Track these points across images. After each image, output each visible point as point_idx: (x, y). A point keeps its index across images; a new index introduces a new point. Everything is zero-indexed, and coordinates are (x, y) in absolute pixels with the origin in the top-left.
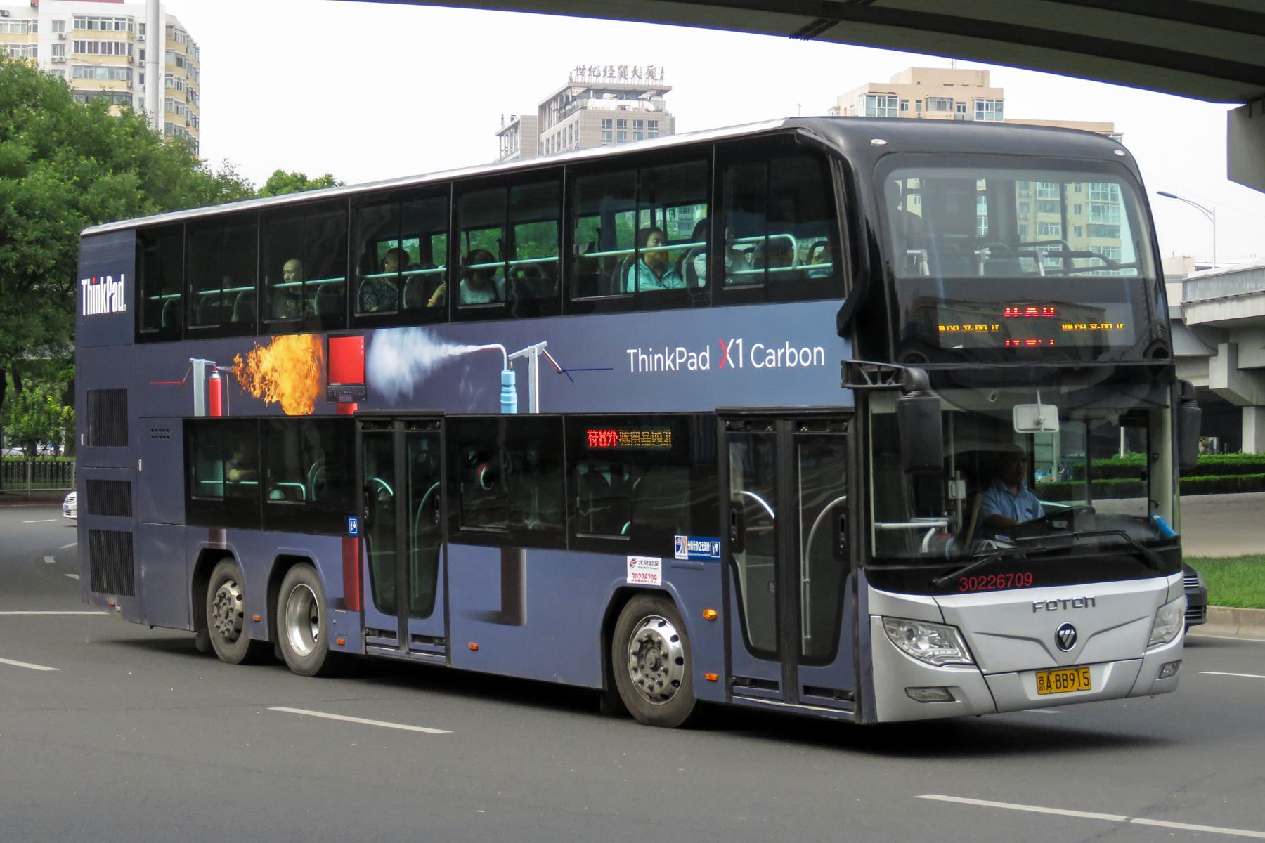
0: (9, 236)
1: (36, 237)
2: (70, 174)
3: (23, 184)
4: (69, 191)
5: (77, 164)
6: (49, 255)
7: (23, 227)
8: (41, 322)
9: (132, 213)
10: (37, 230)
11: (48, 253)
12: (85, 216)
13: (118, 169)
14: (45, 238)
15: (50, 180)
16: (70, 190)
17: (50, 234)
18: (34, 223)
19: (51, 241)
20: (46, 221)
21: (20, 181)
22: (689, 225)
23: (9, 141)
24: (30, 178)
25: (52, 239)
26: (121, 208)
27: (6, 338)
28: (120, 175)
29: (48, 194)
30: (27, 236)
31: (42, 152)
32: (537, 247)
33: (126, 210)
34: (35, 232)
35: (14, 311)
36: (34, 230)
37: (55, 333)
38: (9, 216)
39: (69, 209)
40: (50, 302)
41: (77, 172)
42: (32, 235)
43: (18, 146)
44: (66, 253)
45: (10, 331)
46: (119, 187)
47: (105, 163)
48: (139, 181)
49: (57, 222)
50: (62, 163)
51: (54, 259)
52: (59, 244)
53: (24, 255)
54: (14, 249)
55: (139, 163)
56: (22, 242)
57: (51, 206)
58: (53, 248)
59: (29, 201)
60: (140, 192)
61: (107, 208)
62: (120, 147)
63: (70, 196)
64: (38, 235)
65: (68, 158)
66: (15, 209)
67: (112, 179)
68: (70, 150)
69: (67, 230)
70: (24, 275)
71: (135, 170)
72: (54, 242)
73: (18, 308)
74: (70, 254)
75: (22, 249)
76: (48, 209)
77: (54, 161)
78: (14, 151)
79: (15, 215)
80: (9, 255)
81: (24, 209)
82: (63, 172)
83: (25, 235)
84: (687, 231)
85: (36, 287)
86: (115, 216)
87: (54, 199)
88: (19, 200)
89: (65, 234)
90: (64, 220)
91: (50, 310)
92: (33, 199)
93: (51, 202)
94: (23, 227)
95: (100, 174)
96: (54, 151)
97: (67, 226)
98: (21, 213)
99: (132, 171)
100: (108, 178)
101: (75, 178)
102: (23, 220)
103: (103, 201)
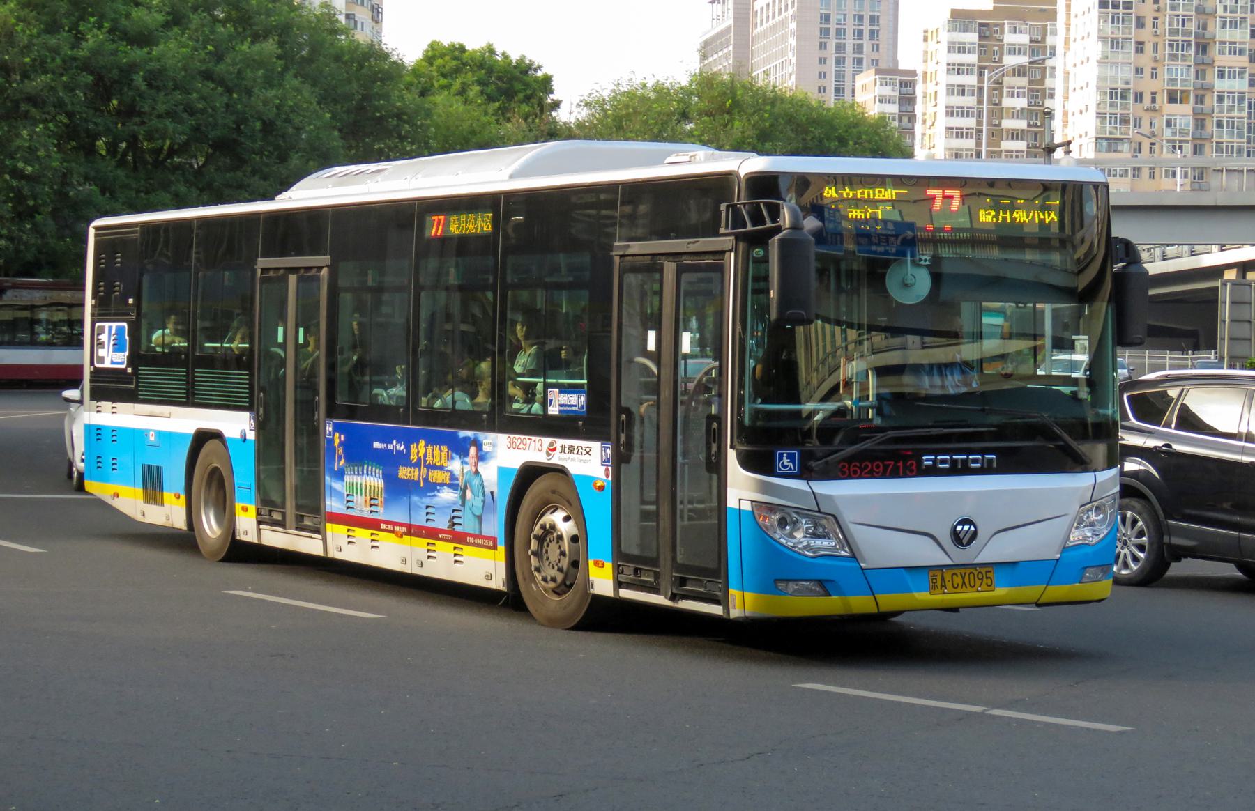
0: (137, 109)
2: (207, 41)
3: (154, 53)
4: (203, 61)
5: (213, 32)
7: (154, 100)
11: (180, 128)
13: (256, 38)
15: (184, 50)
16: (205, 59)
18: (166, 95)
21: (151, 49)
23: (140, 7)
24: (161, 47)
25: (183, 112)
26: (259, 80)
28: (258, 45)
29: (179, 65)
31: (176, 20)
40: (181, 179)
41: (212, 40)
42: (161, 108)
43: (150, 12)
46: (256, 57)
47: (244, 30)
48: (279, 51)
49: (189, 94)
50: (196, 30)
51: (186, 134)
54: (143, 123)
55: (280, 31)
56: (151, 115)
57: (184, 77)
59: (159, 69)
60: (281, 62)
61: (243, 79)
62: (260, 14)
63: (204, 68)
65: (203, 26)
66: (145, 79)
67: (249, 48)
68: (205, 17)
71: (274, 40)
72: (185, 115)
74: (203, 128)
75: (151, 123)
77: (189, 29)
78: (148, 19)
79: (143, 87)
80: (135, 128)
81: (155, 79)
82: (197, 41)
85: (169, 161)
86: (252, 87)
87: (186, 71)
88: (148, 71)
90: (197, 92)
92: (166, 70)
93: (183, 73)
94: (154, 100)
95: (237, 43)
96: (189, 17)
98: (150, 85)
99: (271, 40)
100: (245, 47)
101: (210, 48)
102: (153, 91)
103: (239, 72)
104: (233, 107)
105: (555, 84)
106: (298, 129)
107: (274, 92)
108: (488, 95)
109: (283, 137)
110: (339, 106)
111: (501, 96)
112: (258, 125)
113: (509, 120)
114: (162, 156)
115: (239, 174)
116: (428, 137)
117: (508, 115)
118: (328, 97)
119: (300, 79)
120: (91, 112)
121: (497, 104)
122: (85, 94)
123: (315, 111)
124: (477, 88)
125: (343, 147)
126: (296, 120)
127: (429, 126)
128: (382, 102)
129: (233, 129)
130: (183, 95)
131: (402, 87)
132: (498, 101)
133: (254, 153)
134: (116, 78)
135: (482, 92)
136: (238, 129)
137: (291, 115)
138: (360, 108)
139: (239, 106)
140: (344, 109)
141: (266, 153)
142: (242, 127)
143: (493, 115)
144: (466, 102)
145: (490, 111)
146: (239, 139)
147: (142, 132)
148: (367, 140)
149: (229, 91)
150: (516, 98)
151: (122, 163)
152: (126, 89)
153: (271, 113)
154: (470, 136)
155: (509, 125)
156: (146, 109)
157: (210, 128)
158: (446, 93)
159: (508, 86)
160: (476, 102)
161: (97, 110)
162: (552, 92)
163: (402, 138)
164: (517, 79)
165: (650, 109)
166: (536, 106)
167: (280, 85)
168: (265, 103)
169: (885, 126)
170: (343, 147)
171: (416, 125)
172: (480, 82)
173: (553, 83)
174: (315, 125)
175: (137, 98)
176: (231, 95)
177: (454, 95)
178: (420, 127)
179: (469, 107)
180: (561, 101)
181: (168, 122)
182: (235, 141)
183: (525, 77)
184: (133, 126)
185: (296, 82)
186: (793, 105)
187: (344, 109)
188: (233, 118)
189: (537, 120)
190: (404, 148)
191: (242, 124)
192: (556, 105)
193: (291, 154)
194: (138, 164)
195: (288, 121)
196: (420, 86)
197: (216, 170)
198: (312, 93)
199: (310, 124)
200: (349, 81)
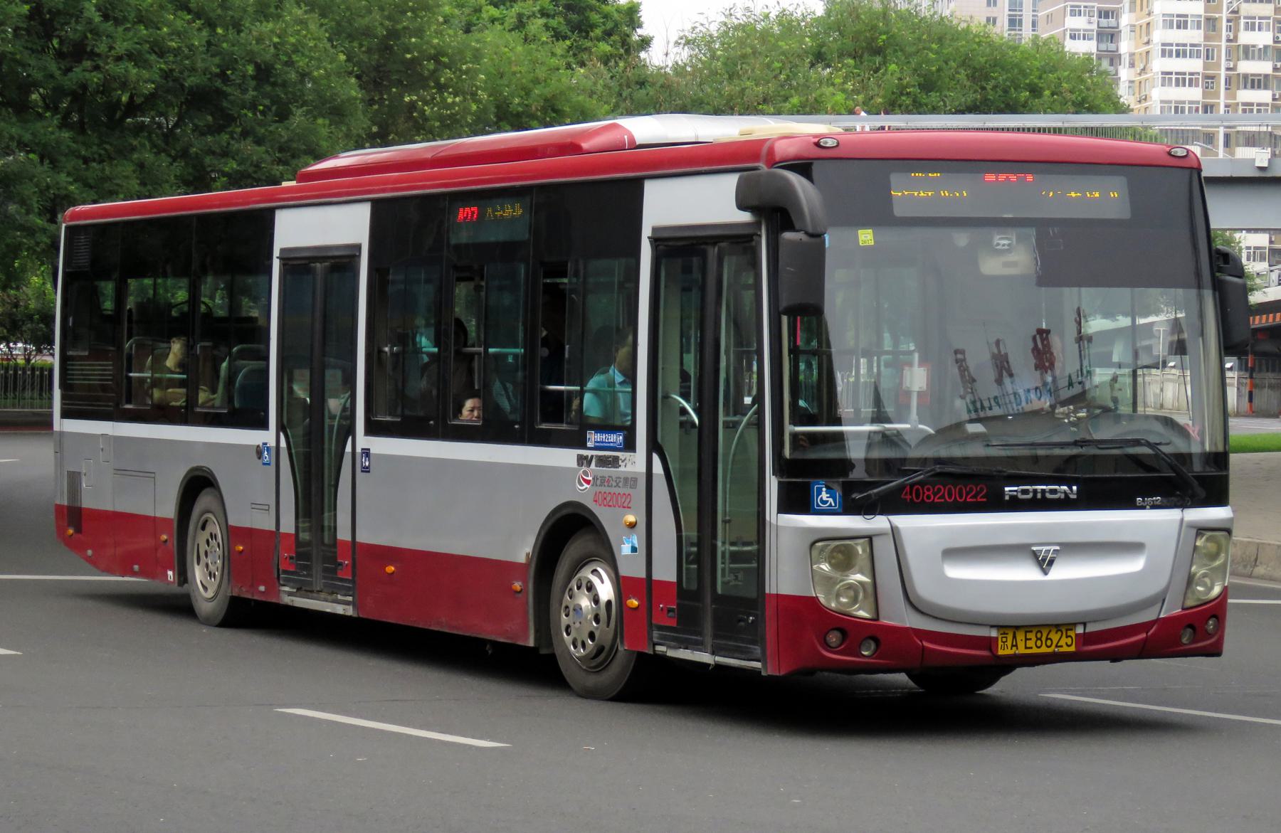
0: (89, 49)
1: (126, 50)
6: (147, 76)
8: (134, 172)
9: (265, 16)
10: (130, 39)
11: (145, 74)
12: (197, 21)
14: (140, 53)
17: (148, 46)
19: (148, 56)
20: (143, 28)
22: (1112, 36)
25: (149, 53)
27: (84, 195)
30: (115, 48)
32: (855, 67)
33: (256, 12)
34: (125, 43)
35: (96, 156)
36: (124, 41)
37: (155, 189)
38: (90, 21)
39: (176, 10)
40: (148, 148)
42: (121, 47)
44: (171, 70)
45: (91, 187)
49: (159, 29)
51: (153, 82)
52: (162, 61)
53: (109, 75)
54: (97, 68)
56: (108, 57)
58: (152, 67)
64: (129, 47)
66: (99, 9)
69: (172, 40)
70: (113, 106)
72: (153, 57)
73: (102, 152)
74: (176, 74)
75: (107, 67)
76: (147, 10)
79: (97, 19)
80: (87, 75)
83: (111, 48)
84: (1109, 44)
85: (129, 120)
86: (241, 19)
89: (169, 48)
90: (169, 26)
91: (148, 156)
94: (111, 37)
97: (172, 34)
98: (106, 17)
102: (109, 26)
104: (216, 45)
105: (645, 15)
106: (303, 76)
107: (271, 25)
108: (553, 29)
109: (284, 85)
110: (355, 44)
111: (573, 33)
112: (250, 69)
113: (582, 64)
114: (118, 115)
115: (225, 137)
116: (477, 88)
117: (585, 56)
118: (342, 32)
119: (304, 8)
120: (26, 53)
121: (568, 42)
122: (16, 30)
123: (325, 49)
124: (541, 21)
125: (362, 100)
126: (301, 62)
127: (477, 72)
128: (413, 40)
129: (217, 75)
130: (151, 30)
131: (441, 19)
132: (570, 39)
133: (243, 107)
134: (61, 7)
135: (547, 27)
136: (222, 75)
137: (294, 56)
138: (385, 48)
139: (225, 45)
140: (363, 49)
141: (261, 108)
142: (229, 72)
143: (562, 56)
144: (526, 40)
145: (559, 51)
146: (225, 88)
147: (95, 80)
148: (394, 90)
149: (211, 25)
150: (592, 34)
151: (65, 124)
152: (73, 21)
153: (268, 57)
154: (531, 85)
155: (582, 71)
156: (102, 48)
157: (186, 73)
158: (499, 27)
159: (582, 17)
160: (539, 40)
161: (33, 51)
162: (640, 26)
163: (441, 88)
164: (592, 8)
165: (775, 47)
166: (619, 45)
167: (279, 17)
168: (259, 40)
169: (1091, 71)
170: (362, 100)
171: (460, 70)
172: (544, 13)
173: (641, 14)
174: (326, 70)
175: (89, 36)
176: (214, 31)
177: (510, 31)
178: (466, 72)
179: (532, 46)
180: (651, 39)
181: (130, 65)
182: (219, 92)
183: (603, 6)
184: (82, 73)
185: (300, 12)
186: (967, 42)
187: (363, 49)
188: (217, 60)
189: (621, 64)
190: (444, 100)
191: (228, 70)
192: (645, 43)
193: (294, 109)
194: (86, 127)
195: (290, 63)
196: (464, 18)
197: (194, 131)
198: (322, 25)
199: (319, 68)
200: (370, 12)
